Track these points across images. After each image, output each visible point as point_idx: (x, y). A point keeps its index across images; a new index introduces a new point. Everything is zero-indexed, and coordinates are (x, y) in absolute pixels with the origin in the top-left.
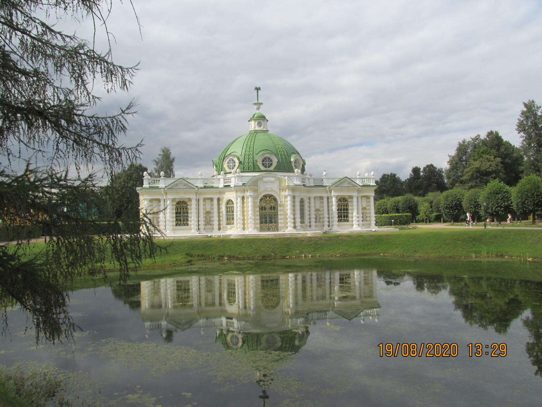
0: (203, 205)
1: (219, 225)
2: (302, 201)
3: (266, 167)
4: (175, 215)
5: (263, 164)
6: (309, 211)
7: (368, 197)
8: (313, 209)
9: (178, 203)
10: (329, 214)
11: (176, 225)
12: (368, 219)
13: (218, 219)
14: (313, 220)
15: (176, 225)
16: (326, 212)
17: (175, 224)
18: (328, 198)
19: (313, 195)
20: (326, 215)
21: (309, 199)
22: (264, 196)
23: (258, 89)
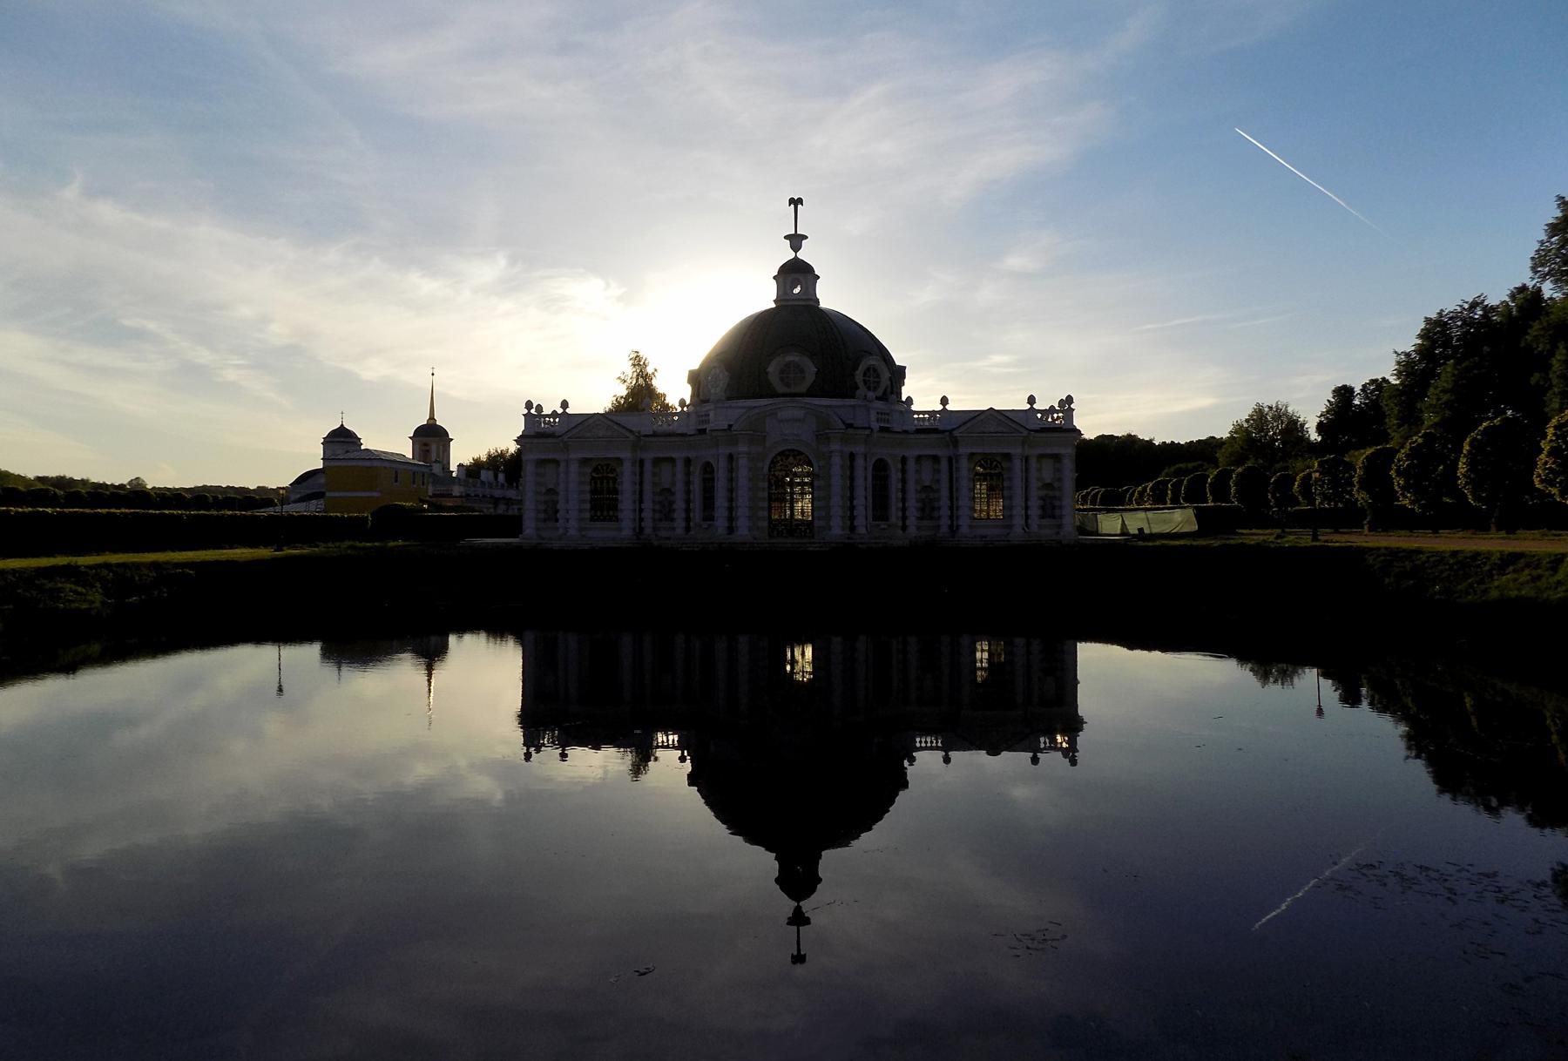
0: (654, 475)
1: (688, 519)
2: (880, 468)
3: (788, 385)
4: (588, 497)
5: (782, 379)
6: (904, 491)
7: (1056, 458)
8: (911, 486)
9: (596, 470)
10: (951, 499)
11: (592, 519)
12: (1057, 512)
13: (684, 506)
14: (913, 514)
15: (592, 519)
16: (945, 493)
17: (588, 515)
18: (950, 460)
19: (911, 453)
20: (944, 501)
21: (904, 460)
22: (781, 454)
23: (796, 202)
